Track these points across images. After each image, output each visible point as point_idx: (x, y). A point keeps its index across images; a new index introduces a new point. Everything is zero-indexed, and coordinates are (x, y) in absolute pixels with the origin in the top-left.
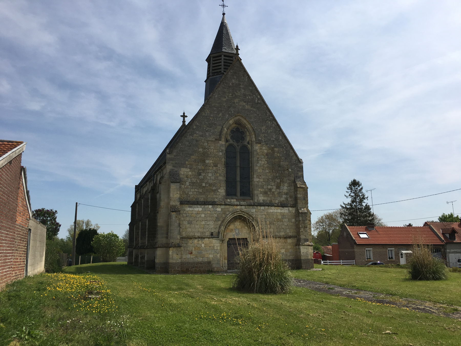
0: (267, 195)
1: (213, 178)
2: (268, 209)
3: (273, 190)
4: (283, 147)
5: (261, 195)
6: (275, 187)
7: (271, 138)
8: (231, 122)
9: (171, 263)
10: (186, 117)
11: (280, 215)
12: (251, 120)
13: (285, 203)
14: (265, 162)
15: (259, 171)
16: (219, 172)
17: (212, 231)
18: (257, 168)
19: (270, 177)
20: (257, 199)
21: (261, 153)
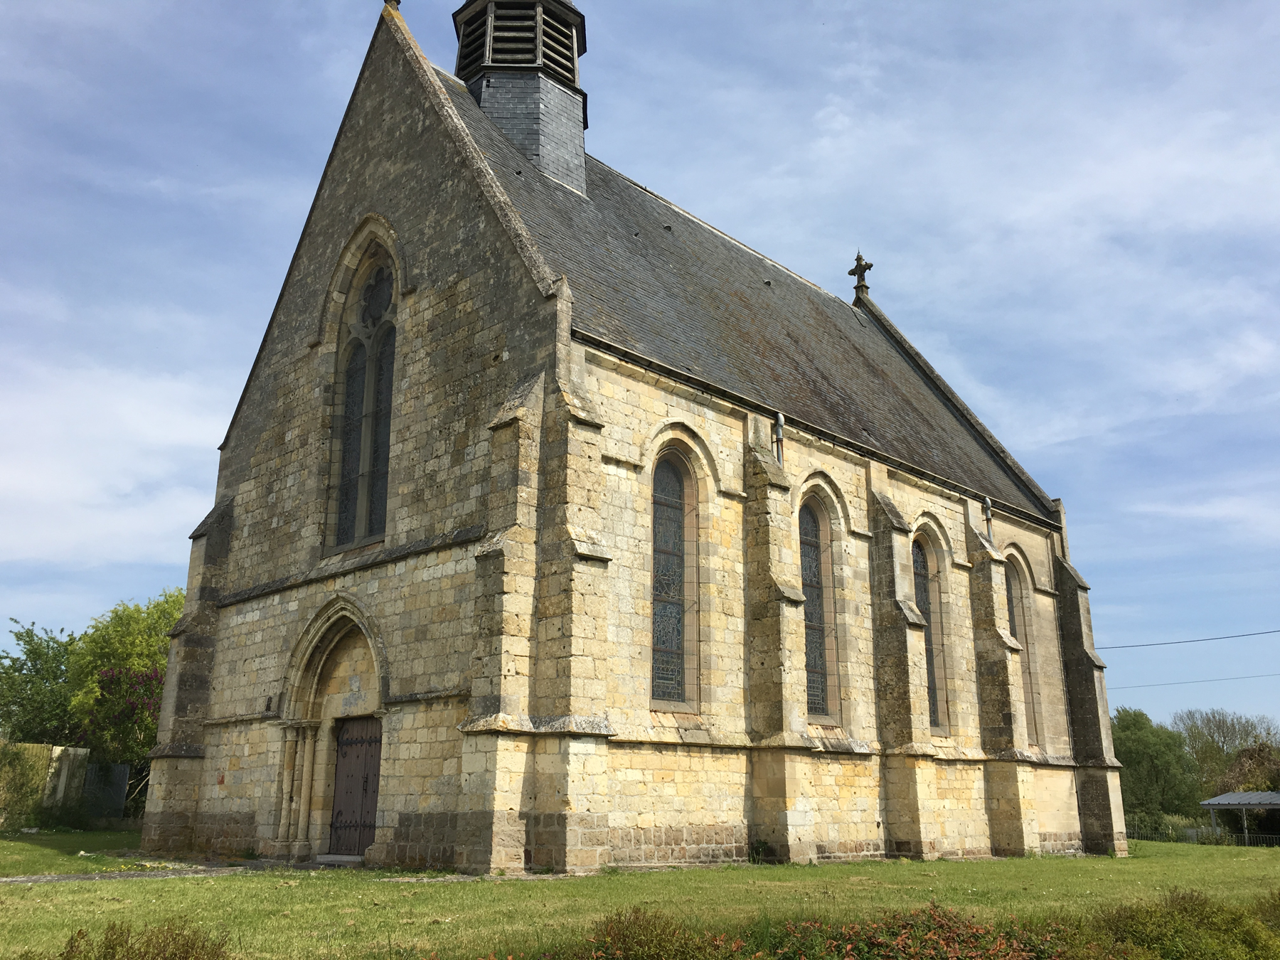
0: (421, 505)
1: (294, 491)
2: (416, 568)
3: (442, 473)
4: (487, 262)
5: (404, 511)
6: (446, 460)
7: (450, 248)
8: (349, 260)
9: (150, 813)
10: (869, 266)
11: (451, 588)
12: (397, 214)
13: (477, 521)
14: (425, 360)
15: (406, 409)
16: (309, 461)
17: (271, 694)
18: (399, 402)
19: (436, 420)
20: (391, 533)
21: (415, 329)
